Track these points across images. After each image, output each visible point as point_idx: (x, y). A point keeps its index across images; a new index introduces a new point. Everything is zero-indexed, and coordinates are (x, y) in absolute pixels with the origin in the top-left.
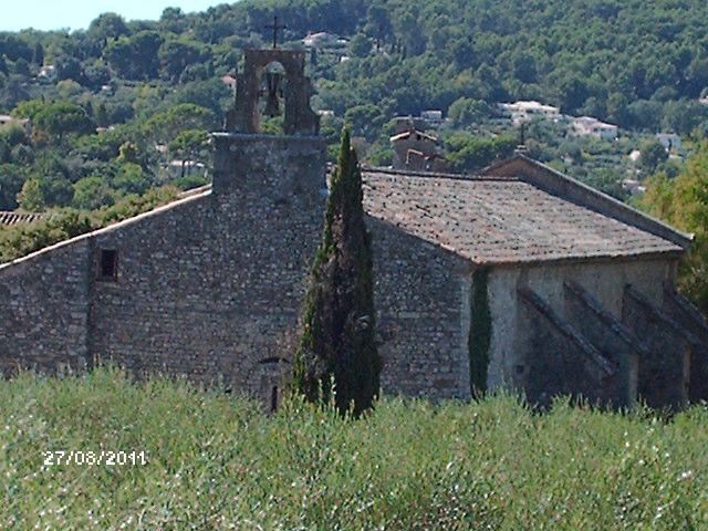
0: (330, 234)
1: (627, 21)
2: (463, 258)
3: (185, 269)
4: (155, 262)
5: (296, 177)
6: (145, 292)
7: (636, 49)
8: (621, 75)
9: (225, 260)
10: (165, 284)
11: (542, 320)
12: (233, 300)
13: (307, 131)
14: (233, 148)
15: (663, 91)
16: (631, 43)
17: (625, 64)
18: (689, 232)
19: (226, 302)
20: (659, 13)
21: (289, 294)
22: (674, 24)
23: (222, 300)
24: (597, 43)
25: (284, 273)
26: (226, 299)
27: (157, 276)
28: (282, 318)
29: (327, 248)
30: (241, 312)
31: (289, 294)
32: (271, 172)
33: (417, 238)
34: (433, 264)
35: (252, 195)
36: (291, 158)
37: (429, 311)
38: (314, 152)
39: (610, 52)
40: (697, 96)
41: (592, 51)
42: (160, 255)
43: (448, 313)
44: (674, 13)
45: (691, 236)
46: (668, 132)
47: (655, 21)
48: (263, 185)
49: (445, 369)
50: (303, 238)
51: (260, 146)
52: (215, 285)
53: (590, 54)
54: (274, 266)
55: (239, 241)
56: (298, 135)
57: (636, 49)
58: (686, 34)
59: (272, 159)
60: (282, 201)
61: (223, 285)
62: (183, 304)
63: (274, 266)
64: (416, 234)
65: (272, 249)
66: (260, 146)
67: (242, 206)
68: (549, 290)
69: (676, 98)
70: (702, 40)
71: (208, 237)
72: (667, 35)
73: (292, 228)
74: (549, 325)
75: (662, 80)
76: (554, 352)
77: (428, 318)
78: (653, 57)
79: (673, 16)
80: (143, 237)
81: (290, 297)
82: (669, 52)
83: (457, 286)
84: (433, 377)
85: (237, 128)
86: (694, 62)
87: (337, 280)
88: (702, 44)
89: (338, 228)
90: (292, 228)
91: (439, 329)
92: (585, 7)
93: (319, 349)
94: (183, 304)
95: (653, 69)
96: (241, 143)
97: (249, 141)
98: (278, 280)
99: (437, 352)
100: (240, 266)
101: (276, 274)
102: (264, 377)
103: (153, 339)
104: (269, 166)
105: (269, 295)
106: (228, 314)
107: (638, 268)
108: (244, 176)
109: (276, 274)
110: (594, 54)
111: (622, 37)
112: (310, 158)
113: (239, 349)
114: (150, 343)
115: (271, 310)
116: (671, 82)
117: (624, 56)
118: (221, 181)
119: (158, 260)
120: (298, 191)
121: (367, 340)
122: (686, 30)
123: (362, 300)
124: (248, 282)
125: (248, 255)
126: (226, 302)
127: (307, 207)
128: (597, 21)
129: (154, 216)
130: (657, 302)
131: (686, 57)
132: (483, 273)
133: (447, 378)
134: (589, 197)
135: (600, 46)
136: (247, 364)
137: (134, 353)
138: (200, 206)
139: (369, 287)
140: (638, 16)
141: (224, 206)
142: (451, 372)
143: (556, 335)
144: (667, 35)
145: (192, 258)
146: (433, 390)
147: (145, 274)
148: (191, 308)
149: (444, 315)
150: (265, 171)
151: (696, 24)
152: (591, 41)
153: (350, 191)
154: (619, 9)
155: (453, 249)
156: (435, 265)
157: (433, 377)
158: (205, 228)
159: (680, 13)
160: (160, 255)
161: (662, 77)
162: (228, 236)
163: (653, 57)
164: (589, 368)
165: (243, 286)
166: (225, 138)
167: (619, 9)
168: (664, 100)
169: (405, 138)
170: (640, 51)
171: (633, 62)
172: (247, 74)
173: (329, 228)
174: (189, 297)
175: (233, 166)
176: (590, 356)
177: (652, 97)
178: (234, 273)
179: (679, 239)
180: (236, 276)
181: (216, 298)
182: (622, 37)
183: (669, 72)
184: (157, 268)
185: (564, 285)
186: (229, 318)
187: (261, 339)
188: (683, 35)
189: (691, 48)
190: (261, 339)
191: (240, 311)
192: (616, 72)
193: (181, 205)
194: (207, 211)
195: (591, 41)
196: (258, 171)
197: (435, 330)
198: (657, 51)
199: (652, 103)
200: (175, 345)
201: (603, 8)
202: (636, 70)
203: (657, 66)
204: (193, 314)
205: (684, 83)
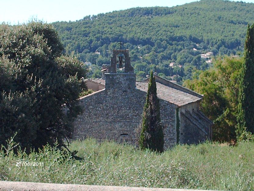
0: (148, 100)
1: (74, 32)
2: (176, 105)
3: (98, 111)
4: (90, 109)
5: (129, 85)
6: (87, 117)
7: (77, 39)
8: (74, 46)
9: (110, 108)
10: (93, 115)
11: (187, 120)
12: (112, 118)
13: (131, 72)
14: (111, 77)
15: (86, 50)
16: (76, 38)
17: (75, 43)
18: (202, 94)
19: (110, 119)
20: (83, 29)
21: (128, 116)
22: (87, 32)
23: (109, 119)
24: (66, 38)
25: (126, 111)
26: (110, 118)
27: (91, 113)
28: (126, 123)
29: (148, 104)
30: (115, 122)
31: (128, 116)
32: (121, 83)
33: (163, 100)
34: (168, 107)
35: (116, 90)
36: (127, 79)
37: (167, 119)
38: (133, 77)
39: (70, 40)
40: (94, 51)
41: (65, 40)
42: (91, 107)
43: (172, 120)
44: (87, 29)
45: (203, 95)
46: (88, 62)
47: (82, 31)
48: (119, 87)
49: (172, 135)
50: (131, 101)
51: (118, 76)
52: (107, 114)
53: (65, 41)
54: (123, 109)
55: (113, 102)
56: (129, 73)
57: (77, 39)
58: (91, 35)
59: (122, 80)
60: (125, 91)
61: (109, 114)
62: (98, 120)
63: (123, 109)
64: (162, 99)
65: (123, 104)
66: (118, 76)
67: (113, 93)
68: (183, 111)
69: (89, 53)
70: (95, 36)
71: (105, 101)
72: (86, 35)
73: (128, 98)
74: (189, 121)
75: (85, 47)
76: (191, 129)
77: (166, 121)
78: (82, 41)
79: (87, 30)
80: (86, 102)
81: (128, 117)
82: (86, 40)
83: (174, 112)
84: (169, 137)
85: (111, 72)
86: (93, 42)
87: (152, 113)
88: (96, 37)
89: (151, 98)
90: (128, 98)
91: (170, 124)
92: (62, 28)
93: (148, 131)
94: (98, 120)
95: (83, 44)
96: (113, 76)
97: (115, 75)
98: (124, 112)
99: (169, 131)
100: (114, 109)
101: (124, 111)
102: (121, 139)
103: (90, 130)
104: (121, 82)
105: (122, 117)
106: (111, 122)
107: (194, 105)
108: (114, 85)
109: (124, 111)
110: (66, 41)
111: (74, 36)
112: (132, 79)
113: (114, 132)
114: (89, 131)
115: (123, 121)
116: (88, 48)
117: (74, 41)
118: (107, 86)
119: (91, 109)
120: (129, 88)
121: (160, 129)
122: (90, 34)
123: (158, 118)
124: (116, 113)
125: (116, 106)
126: (110, 119)
127: (132, 93)
128: (66, 32)
129: (89, 96)
130: (191, 112)
131: (91, 41)
132: (178, 108)
133: (172, 137)
134: (175, 86)
135: (68, 39)
136: (117, 136)
137: (85, 134)
138: (102, 93)
139: (159, 114)
140: (78, 30)
141: (109, 93)
142: (173, 136)
143: (191, 124)
144: (86, 35)
145: (100, 107)
146: (169, 141)
147: (87, 112)
148: (101, 121)
149: (171, 121)
150: (120, 83)
151: (93, 32)
152: (65, 37)
153: (153, 89)
154: (72, 28)
155: (173, 103)
156: (168, 107)
157: (169, 137)
158: (104, 99)
159: (89, 29)
160: (91, 107)
161: (85, 47)
162: (110, 101)
163: (82, 41)
164: (201, 133)
165: (115, 114)
166: (108, 74)
167: (72, 28)
168: (86, 53)
169: (106, 70)
170: (79, 40)
171: (77, 43)
172: (114, 57)
173: (148, 98)
174: (100, 118)
175: (111, 82)
176: (201, 130)
177: (83, 52)
178: (112, 111)
179: (200, 96)
180: (113, 112)
181: (107, 118)
182: (74, 36)
183: (87, 46)
184: (90, 110)
185: (185, 110)
186: (111, 123)
187: (120, 129)
188: (90, 35)
189: (93, 39)
190: (120, 129)
191: (114, 121)
192: (72, 46)
193: (96, 93)
194: (104, 95)
195: (65, 37)
196: (118, 83)
197: (168, 125)
198: (83, 39)
199: (83, 54)
200: (97, 131)
201: (67, 28)
202: (78, 45)
203: (83, 44)
204: (101, 123)
205: (91, 48)
